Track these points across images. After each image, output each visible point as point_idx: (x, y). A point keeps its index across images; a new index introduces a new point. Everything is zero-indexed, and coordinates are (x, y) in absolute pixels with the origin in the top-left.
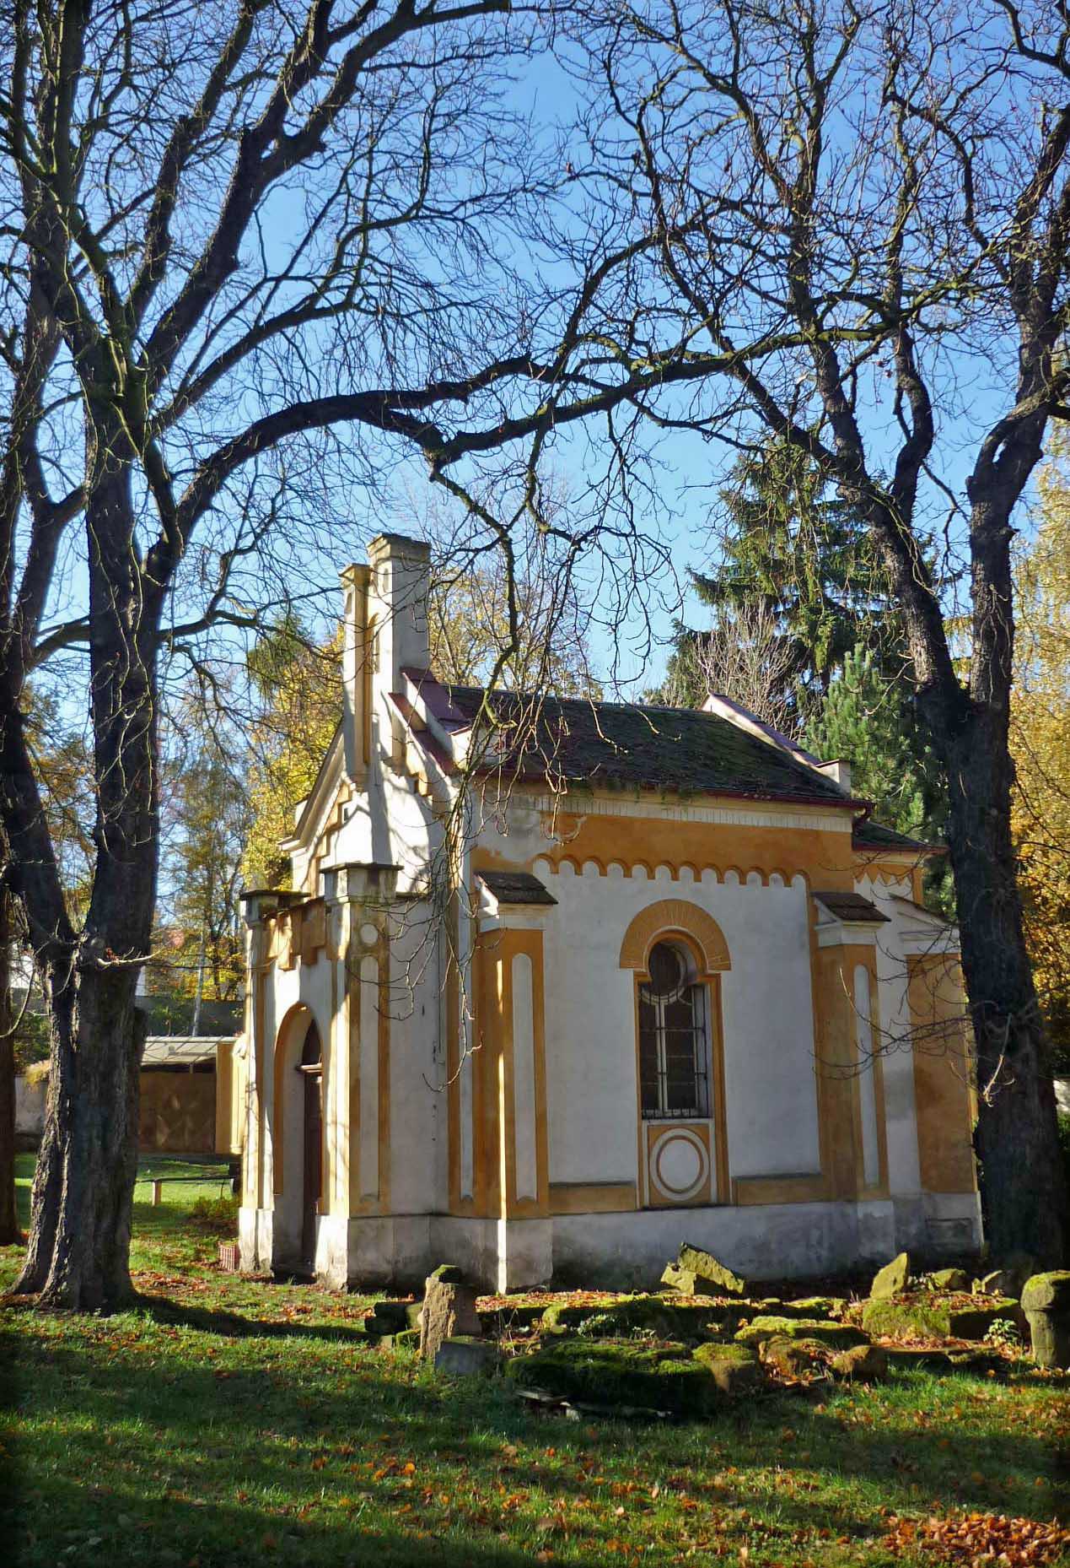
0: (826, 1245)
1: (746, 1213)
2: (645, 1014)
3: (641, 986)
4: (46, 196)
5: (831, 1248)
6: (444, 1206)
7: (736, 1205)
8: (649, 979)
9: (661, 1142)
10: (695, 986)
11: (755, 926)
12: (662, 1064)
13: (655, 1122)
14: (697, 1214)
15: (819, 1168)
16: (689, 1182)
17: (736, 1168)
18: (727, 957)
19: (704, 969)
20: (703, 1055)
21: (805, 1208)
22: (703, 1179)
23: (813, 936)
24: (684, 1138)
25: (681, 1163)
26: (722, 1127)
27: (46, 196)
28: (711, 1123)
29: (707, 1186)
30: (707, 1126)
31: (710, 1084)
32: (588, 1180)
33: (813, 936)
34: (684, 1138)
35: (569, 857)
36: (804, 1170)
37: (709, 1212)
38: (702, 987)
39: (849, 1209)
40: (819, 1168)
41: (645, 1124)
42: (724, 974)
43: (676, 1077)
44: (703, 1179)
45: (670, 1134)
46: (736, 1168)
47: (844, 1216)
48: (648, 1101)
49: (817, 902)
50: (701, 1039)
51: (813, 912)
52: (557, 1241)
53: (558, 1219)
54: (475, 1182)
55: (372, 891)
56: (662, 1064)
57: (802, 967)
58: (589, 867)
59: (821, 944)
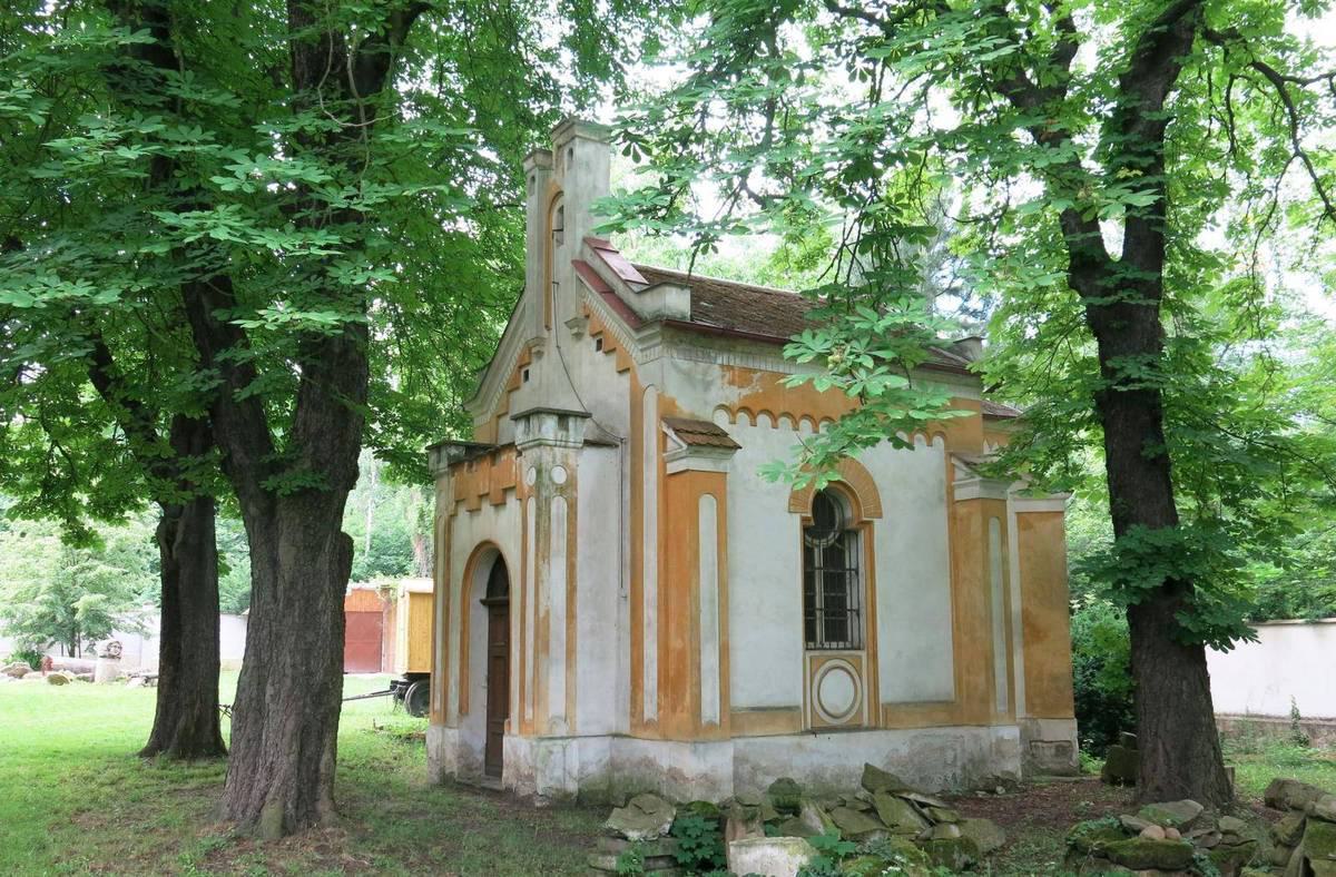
0: (959, 764)
1: (892, 735)
2: (808, 553)
3: (806, 530)
4: (618, 136)
5: (964, 768)
6: (626, 729)
7: (886, 728)
8: (812, 523)
9: (821, 671)
10: (849, 532)
11: (904, 484)
12: (819, 602)
13: (817, 653)
14: (854, 736)
15: (953, 697)
16: (844, 709)
17: (885, 696)
18: (879, 506)
19: (859, 516)
20: (855, 595)
21: (942, 731)
22: (857, 705)
23: (951, 491)
24: (842, 668)
25: (837, 691)
26: (874, 657)
27: (618, 136)
28: (863, 654)
29: (860, 712)
30: (860, 657)
31: (863, 618)
32: (777, 705)
33: (951, 491)
34: (842, 668)
35: (744, 409)
36: (942, 698)
37: (863, 735)
38: (855, 533)
39: (982, 732)
40: (953, 697)
41: (809, 654)
42: (877, 522)
43: (831, 611)
44: (857, 705)
45: (828, 664)
46: (885, 696)
47: (977, 738)
48: (810, 634)
49: (954, 461)
50: (854, 582)
51: (951, 469)
52: (738, 760)
53: (738, 741)
54: (659, 707)
55: (561, 434)
56: (819, 602)
57: (942, 514)
58: (763, 419)
59: (957, 498)
